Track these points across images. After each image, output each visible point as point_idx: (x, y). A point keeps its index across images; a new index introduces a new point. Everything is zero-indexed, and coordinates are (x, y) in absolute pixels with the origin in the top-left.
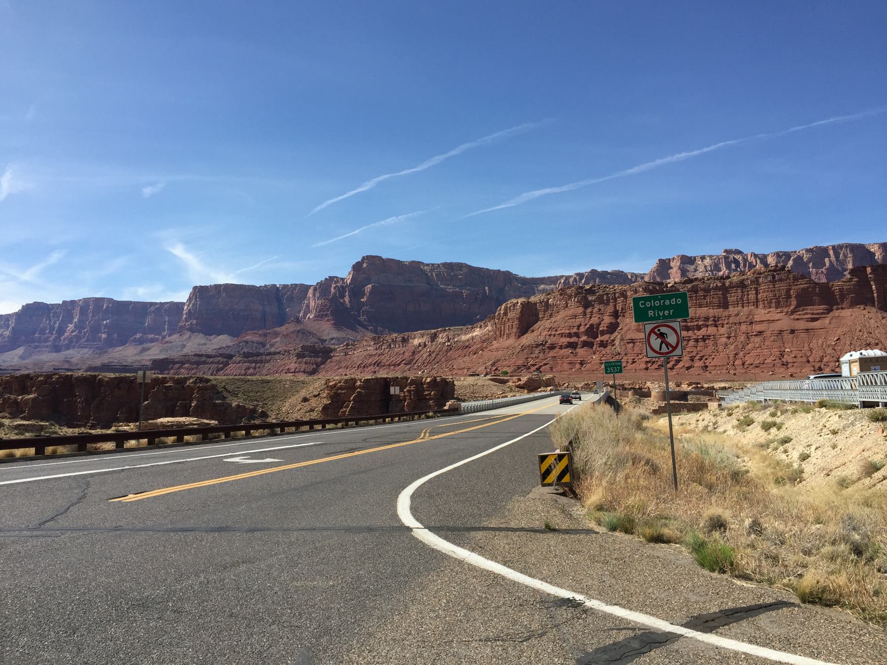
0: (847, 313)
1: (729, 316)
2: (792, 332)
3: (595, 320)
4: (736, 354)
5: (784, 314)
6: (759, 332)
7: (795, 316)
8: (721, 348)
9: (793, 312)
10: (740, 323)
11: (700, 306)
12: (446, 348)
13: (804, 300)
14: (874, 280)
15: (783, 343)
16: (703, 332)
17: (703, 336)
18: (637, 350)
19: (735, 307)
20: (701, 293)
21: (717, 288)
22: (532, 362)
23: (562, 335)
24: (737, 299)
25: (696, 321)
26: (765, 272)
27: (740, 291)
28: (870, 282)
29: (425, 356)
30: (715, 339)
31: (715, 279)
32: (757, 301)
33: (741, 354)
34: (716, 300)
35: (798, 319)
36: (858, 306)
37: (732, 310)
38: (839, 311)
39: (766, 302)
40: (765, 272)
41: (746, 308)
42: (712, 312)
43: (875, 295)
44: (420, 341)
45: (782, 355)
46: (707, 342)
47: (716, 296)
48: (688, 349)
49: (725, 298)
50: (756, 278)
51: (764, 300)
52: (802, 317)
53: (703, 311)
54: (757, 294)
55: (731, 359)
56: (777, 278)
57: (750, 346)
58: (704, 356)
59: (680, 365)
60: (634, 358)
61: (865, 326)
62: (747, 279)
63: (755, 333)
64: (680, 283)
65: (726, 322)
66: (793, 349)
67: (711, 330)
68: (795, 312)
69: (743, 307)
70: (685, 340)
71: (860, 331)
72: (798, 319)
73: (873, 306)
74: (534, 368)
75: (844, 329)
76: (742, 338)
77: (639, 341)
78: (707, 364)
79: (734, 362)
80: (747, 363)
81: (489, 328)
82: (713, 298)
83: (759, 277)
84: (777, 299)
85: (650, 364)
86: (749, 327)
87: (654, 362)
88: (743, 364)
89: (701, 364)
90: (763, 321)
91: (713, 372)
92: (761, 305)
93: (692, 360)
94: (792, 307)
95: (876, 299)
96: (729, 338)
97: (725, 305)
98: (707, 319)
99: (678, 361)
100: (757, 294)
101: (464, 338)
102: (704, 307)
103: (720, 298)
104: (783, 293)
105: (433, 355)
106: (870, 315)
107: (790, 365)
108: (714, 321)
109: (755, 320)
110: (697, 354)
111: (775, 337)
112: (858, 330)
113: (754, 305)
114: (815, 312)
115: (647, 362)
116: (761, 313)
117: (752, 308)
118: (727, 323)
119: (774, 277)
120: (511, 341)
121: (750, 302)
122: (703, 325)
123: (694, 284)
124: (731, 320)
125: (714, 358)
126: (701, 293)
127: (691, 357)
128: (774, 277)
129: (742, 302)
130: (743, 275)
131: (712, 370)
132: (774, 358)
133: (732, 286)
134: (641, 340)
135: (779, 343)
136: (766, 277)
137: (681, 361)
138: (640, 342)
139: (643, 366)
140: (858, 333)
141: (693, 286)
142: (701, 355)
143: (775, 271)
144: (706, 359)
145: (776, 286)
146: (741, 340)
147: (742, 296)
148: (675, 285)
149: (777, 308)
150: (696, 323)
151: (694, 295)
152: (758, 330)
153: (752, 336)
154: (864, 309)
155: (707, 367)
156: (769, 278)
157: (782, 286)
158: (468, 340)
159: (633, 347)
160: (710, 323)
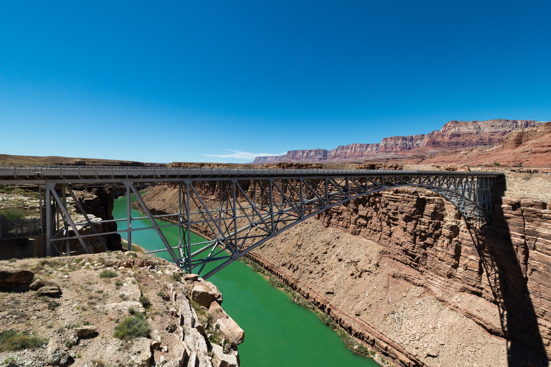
12: (477, 155)
22: (518, 159)
23: (543, 146)
29: (466, 158)
44: (464, 152)
74: (519, 163)
81: (501, 145)
105: (470, 158)
120: (509, 151)
158: (490, 151)
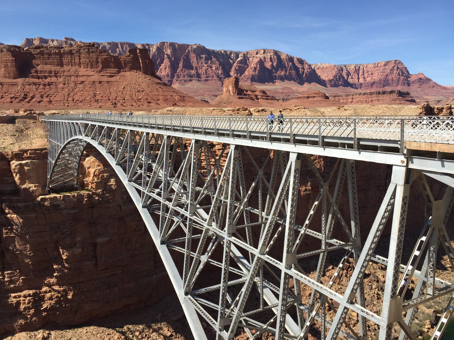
0: (128, 74)
1: (64, 71)
2: (100, 82)
4: (69, 94)
5: (95, 72)
6: (82, 82)
7: (101, 74)
8: (59, 90)
9: (100, 72)
10: (71, 76)
11: (46, 64)
13: (106, 65)
14: (141, 57)
15: (96, 89)
16: (48, 80)
17: (49, 83)
18: (4, 89)
19: (67, 66)
20: (46, 56)
21: (55, 53)
24: (68, 61)
25: (44, 73)
26: (83, 47)
27: (70, 56)
28: (138, 58)
30: (56, 85)
31: (54, 48)
32: (80, 64)
33: (72, 94)
34: (55, 61)
35: (103, 76)
36: (133, 71)
37: (66, 68)
38: (124, 72)
39: (85, 64)
40: (83, 47)
41: (74, 67)
42: (53, 68)
43: (141, 65)
45: (95, 96)
46: (51, 86)
47: (55, 59)
48: (39, 90)
49: (61, 60)
50: (79, 49)
51: (84, 63)
52: (105, 74)
53: (48, 67)
54: (80, 59)
55: (66, 97)
56: (91, 50)
57: (77, 90)
58: (49, 95)
59: (34, 100)
60: (2, 95)
61: (137, 81)
62: (74, 50)
63: (79, 82)
64: (32, 48)
65: (62, 75)
66: (101, 92)
67: (53, 79)
68: (101, 71)
69: (72, 66)
70: (37, 84)
71: (135, 84)
72: (103, 76)
73: (141, 71)
75: (127, 83)
76: (72, 85)
77: (6, 84)
78: (51, 100)
79: (68, 99)
80: (75, 99)
82: (54, 59)
83: (80, 49)
84: (91, 63)
85: (14, 99)
86: (76, 78)
87: (17, 98)
88: (73, 100)
89: (47, 99)
90: (84, 75)
91: (55, 105)
92: (82, 66)
93: (42, 97)
94: (100, 69)
95: (142, 67)
96: (64, 84)
97: (62, 65)
98: (50, 72)
99: (33, 98)
100: (80, 59)
102: (49, 65)
103: (58, 60)
104: (94, 60)
106: (140, 76)
107: (99, 101)
108: (55, 73)
109: (79, 74)
110: (45, 93)
111: (91, 85)
112: (134, 83)
113: (78, 66)
114: (112, 72)
115: (11, 98)
116: (82, 71)
117: (77, 67)
118: (63, 76)
119: (89, 50)
121: (76, 64)
122: (48, 76)
123: (41, 49)
124: (65, 74)
125: (55, 96)
126: (46, 56)
127: (41, 95)
128: (89, 50)
129: (71, 63)
130: (71, 47)
131: (55, 103)
132: (90, 97)
133: (65, 53)
134: (7, 84)
135: (93, 89)
136: (84, 49)
137: (35, 97)
138: (6, 85)
139: (9, 100)
140: (133, 85)
141: (40, 51)
142: (47, 94)
143: (89, 46)
144: (51, 97)
145: (90, 55)
146: (71, 86)
147: (71, 60)
148: (29, 49)
149: (91, 68)
150: (44, 74)
151: (42, 57)
152: (81, 81)
153: (78, 84)
154: (136, 72)
155: (51, 101)
156: (86, 50)
157: (94, 56)
159: (2, 88)
160: (53, 75)
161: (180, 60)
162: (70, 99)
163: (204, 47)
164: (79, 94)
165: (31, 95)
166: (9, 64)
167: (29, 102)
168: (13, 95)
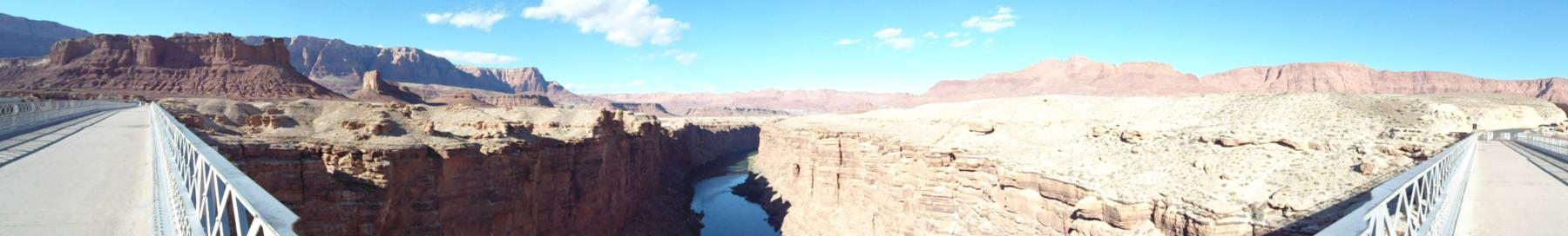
3: (116, 56)
32: (215, 53)
54: (215, 48)
59: (165, 87)
101: (35, 64)
139: (142, 87)
161: (319, 53)
162: (199, 87)
163: (342, 43)
164: (209, 83)
165: (164, 82)
166: (149, 53)
167: (160, 90)
168: (146, 82)
